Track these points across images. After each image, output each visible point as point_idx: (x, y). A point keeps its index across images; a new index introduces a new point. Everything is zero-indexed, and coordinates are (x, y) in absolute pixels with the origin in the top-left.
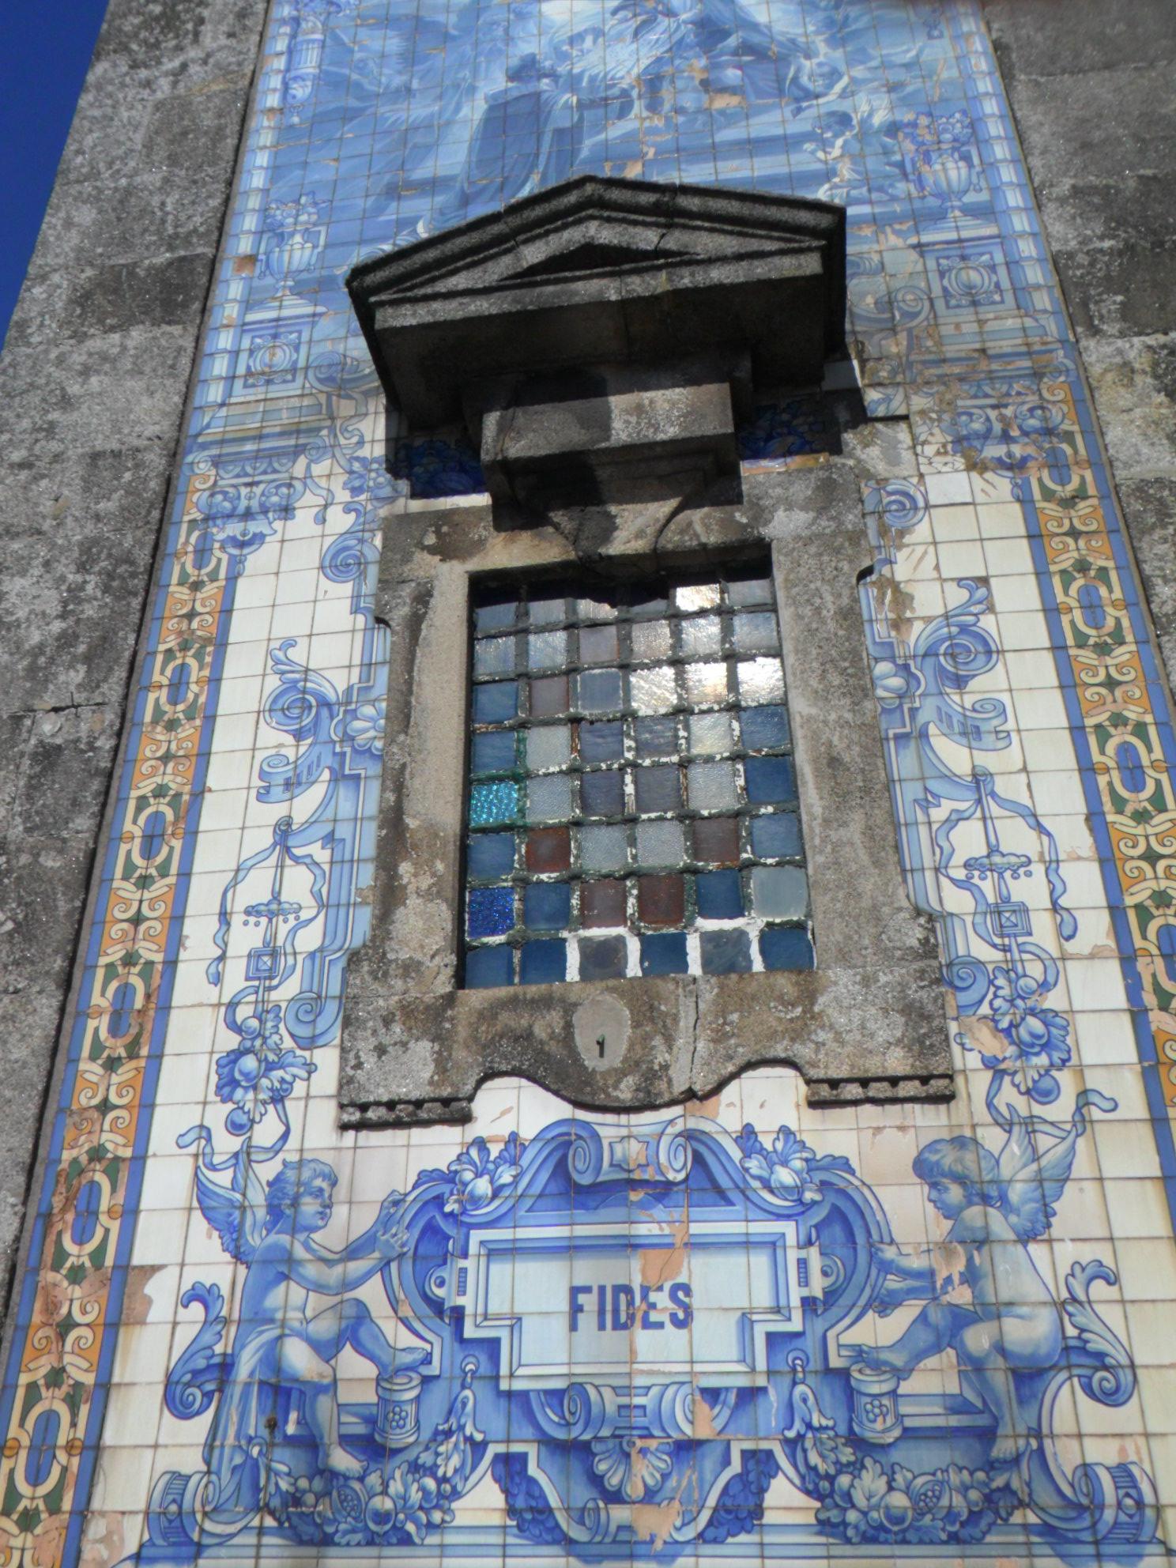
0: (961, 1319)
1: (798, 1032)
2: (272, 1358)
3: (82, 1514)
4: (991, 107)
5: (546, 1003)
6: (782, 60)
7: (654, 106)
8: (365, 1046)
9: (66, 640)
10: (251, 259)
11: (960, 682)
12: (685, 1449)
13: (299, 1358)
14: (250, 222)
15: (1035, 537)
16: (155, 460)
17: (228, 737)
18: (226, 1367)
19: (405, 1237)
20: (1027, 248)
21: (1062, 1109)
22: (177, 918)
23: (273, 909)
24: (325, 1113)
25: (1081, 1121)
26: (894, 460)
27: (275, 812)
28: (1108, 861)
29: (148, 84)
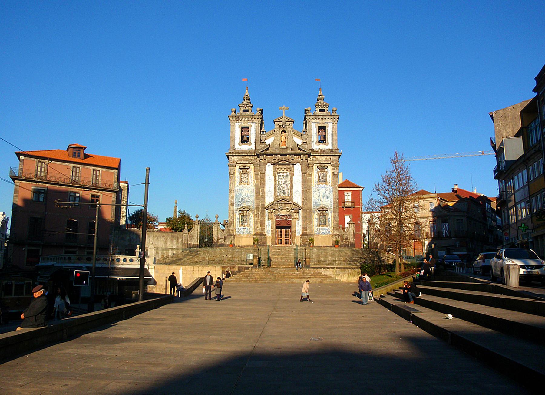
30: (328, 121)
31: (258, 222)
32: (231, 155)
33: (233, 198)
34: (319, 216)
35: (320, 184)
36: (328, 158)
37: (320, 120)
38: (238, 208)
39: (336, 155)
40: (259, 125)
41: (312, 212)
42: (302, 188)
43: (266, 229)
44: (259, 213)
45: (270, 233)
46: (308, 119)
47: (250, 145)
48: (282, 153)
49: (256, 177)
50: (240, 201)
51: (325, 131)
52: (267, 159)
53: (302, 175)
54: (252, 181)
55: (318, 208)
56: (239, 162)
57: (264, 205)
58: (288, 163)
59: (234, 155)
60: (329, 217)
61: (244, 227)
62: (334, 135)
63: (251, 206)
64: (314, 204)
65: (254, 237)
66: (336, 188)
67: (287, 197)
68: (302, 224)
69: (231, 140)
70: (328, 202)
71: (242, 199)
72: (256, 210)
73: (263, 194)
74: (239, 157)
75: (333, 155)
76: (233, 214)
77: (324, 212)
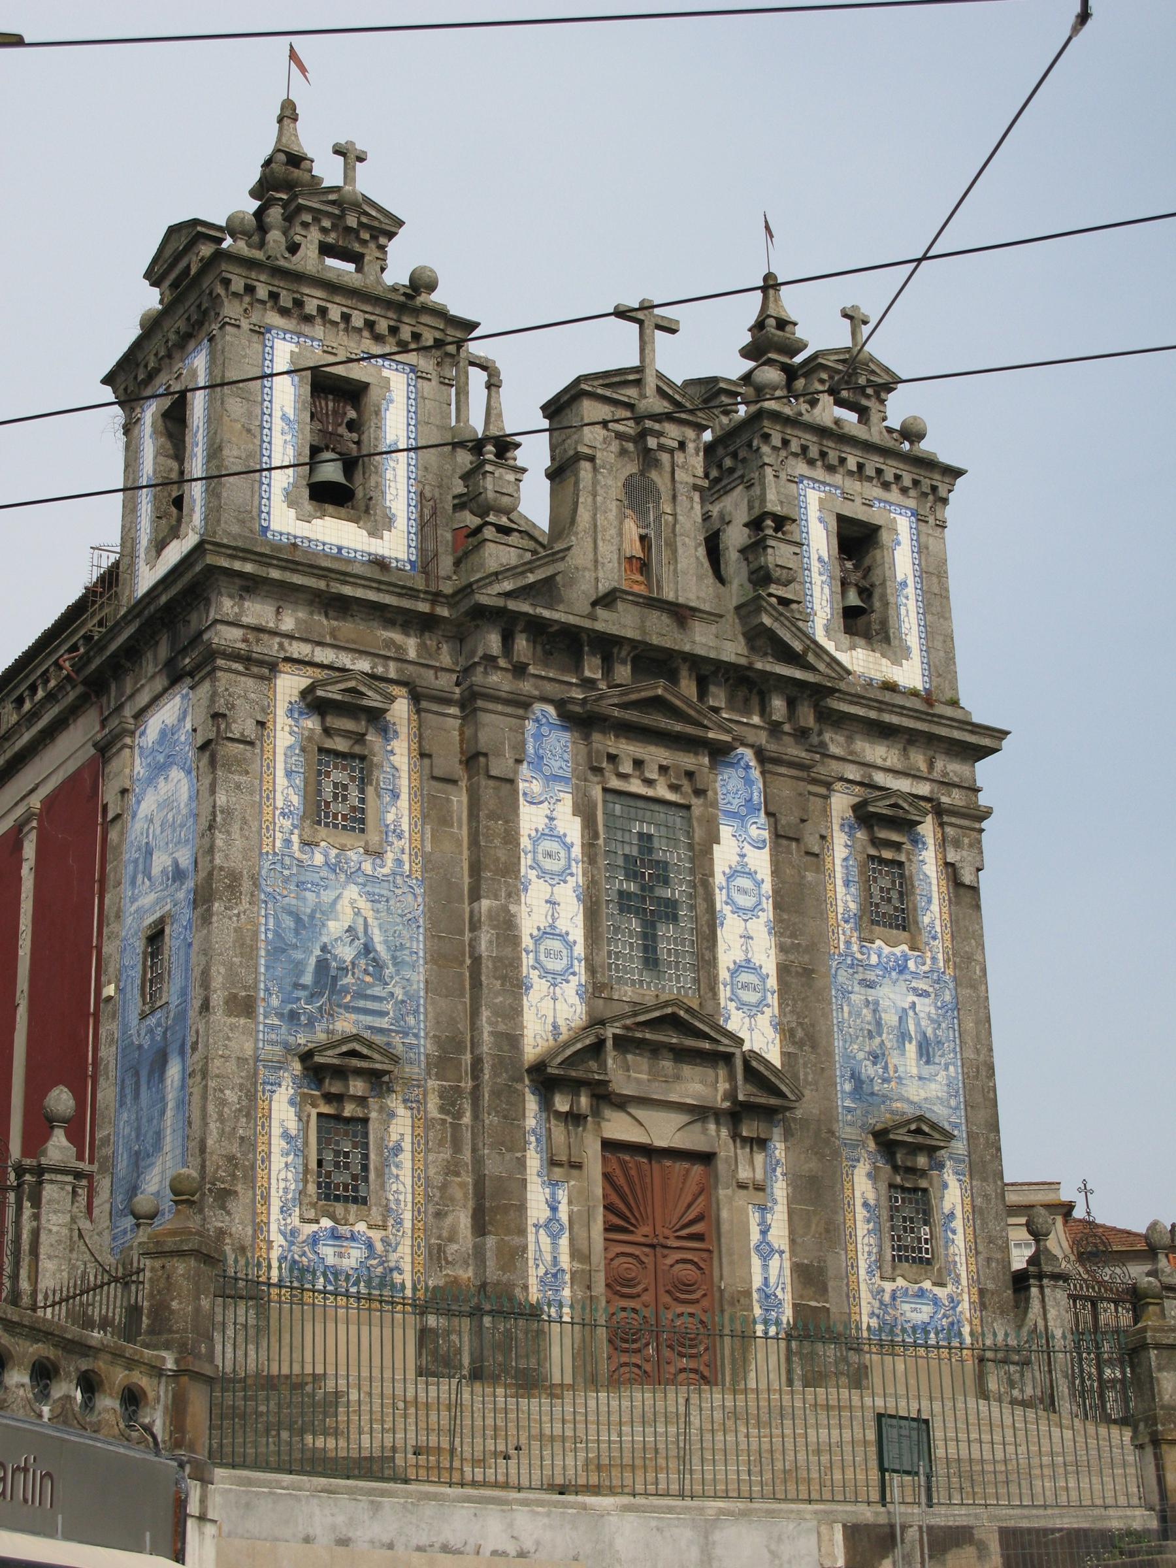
0: (384, 1262)
1: (367, 1216)
2: (293, 1257)
4: (422, 1001)
7: (353, 974)
8: (304, 1208)
9: (240, 1110)
10: (264, 999)
13: (296, 1257)
14: (262, 986)
15: (413, 1127)
16: (251, 1062)
17: (274, 1141)
19: (310, 1241)
20: (422, 1050)
21: (400, 1234)
22: (269, 1179)
23: (286, 1180)
24: (298, 1219)
28: (413, 1194)
29: (230, 918)
30: (894, 495)
31: (459, 1194)
32: (248, 568)
33: (249, 950)
34: (883, 1187)
35: (878, 942)
36: (919, 760)
37: (850, 473)
38: (288, 1048)
41: (836, 1154)
42: (782, 948)
43: (531, 1255)
44: (459, 1115)
45: (567, 1293)
46: (776, 440)
47: (374, 533)
48: (655, 640)
50: (308, 979)
52: (532, 670)
54: (405, 827)
56: (299, 650)
57: (512, 1040)
58: (690, 730)
59: (275, 574)
61: (343, 1230)
63: (397, 1040)
64: (848, 1087)
65: (432, 1321)
66: (974, 987)
68: (792, 1242)
71: (322, 966)
72: (432, 1084)
73: (508, 952)
75: (957, 735)
76: (252, 1097)
77: (922, 1161)
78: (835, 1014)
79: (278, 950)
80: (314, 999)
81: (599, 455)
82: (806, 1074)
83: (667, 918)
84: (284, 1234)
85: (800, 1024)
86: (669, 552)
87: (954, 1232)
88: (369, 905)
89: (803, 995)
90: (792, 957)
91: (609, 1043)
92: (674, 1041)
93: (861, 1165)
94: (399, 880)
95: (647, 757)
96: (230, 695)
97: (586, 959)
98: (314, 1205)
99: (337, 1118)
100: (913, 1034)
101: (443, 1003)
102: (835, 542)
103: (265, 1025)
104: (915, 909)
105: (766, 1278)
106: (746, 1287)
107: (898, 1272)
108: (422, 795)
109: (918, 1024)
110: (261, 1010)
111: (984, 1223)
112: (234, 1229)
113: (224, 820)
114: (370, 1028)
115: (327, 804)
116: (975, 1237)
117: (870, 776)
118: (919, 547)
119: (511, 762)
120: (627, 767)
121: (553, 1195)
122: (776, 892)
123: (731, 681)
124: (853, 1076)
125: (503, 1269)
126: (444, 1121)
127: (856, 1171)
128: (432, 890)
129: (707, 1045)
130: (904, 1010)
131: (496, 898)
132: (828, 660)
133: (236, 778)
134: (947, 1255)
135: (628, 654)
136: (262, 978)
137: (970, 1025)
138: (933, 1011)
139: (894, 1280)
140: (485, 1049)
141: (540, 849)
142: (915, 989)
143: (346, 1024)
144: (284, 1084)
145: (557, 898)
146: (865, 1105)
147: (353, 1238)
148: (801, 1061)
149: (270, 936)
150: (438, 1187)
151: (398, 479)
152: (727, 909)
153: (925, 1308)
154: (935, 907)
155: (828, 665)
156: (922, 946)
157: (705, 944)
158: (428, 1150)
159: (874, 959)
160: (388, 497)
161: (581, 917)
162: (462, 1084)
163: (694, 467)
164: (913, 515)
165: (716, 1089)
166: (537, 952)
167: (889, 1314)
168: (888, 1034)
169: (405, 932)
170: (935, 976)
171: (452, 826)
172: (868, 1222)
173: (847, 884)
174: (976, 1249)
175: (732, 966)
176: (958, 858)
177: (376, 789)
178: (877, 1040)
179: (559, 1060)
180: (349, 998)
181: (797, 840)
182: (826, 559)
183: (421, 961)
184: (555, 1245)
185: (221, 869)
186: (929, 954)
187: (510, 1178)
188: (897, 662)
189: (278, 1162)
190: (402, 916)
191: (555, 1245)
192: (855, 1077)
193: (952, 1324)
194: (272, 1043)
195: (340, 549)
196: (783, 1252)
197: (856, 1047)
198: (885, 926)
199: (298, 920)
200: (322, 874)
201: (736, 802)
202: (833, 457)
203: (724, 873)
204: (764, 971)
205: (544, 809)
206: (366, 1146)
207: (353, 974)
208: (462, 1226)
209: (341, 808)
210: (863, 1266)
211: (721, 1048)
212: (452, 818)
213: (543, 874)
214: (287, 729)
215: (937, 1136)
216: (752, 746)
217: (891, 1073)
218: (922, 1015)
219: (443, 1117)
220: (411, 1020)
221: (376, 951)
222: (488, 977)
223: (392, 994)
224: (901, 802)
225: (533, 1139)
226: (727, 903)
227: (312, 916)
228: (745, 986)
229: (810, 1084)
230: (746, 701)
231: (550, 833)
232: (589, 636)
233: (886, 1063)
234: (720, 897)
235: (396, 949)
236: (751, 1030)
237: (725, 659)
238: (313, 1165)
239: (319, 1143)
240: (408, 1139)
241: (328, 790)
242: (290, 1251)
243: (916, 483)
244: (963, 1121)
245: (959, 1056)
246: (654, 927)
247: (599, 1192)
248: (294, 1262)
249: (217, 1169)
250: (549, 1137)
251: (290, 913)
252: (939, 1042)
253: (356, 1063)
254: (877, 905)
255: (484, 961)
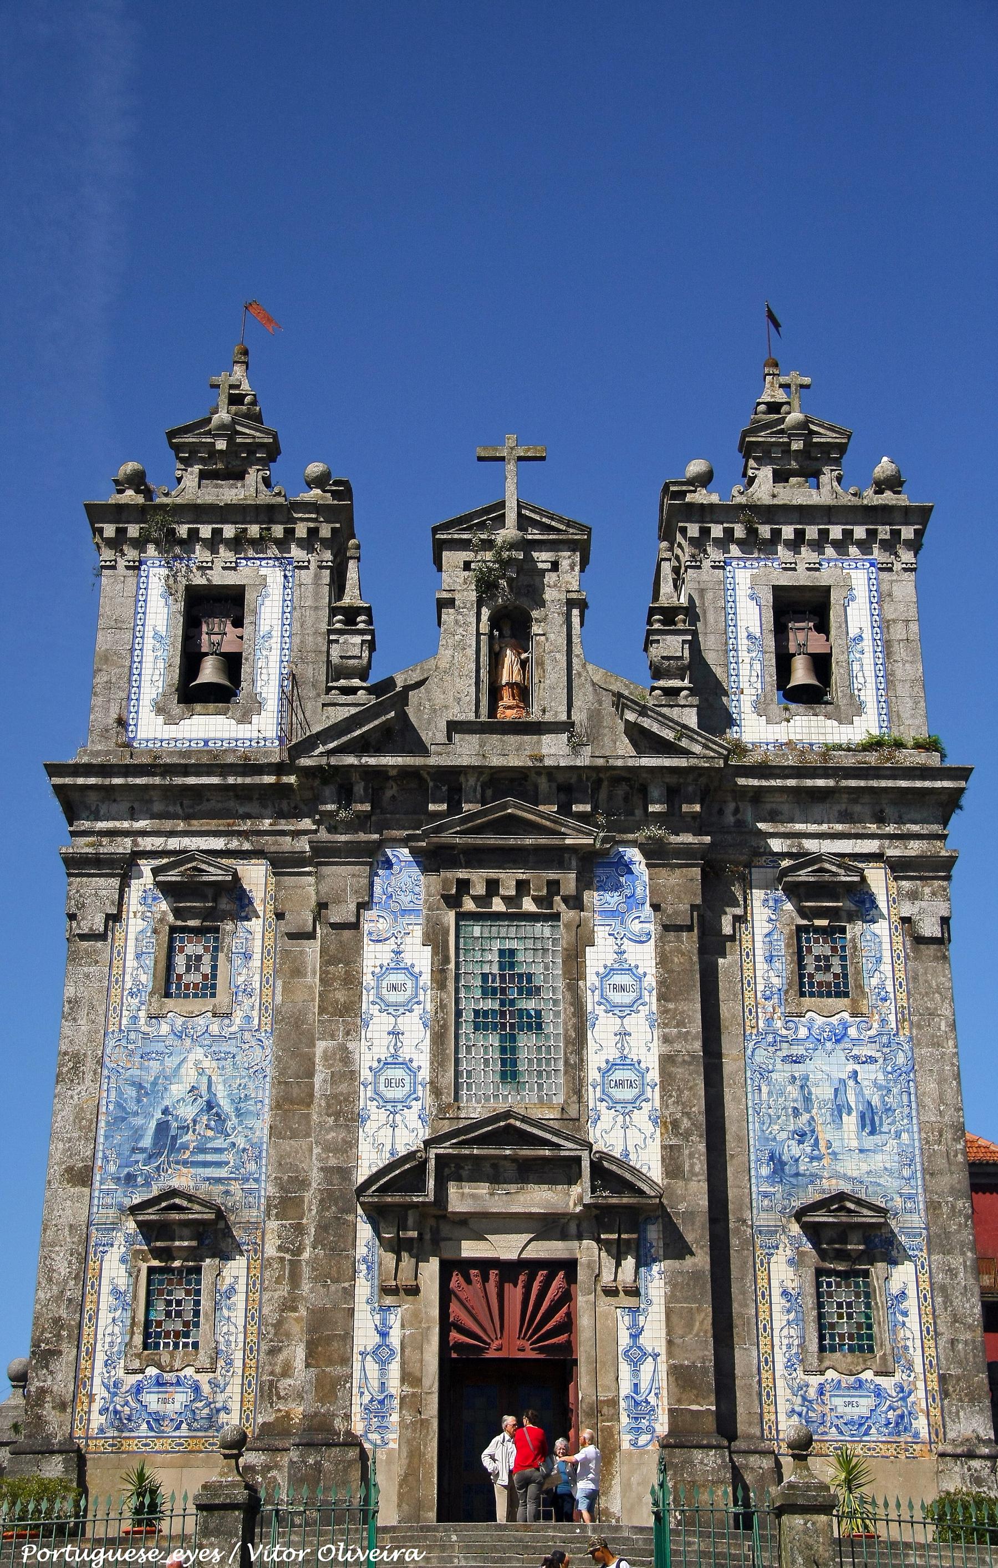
0: (211, 1403)
1: (194, 1361)
2: (115, 1407)
3: (88, 1428)
5: (156, 1354)
6: (224, 1121)
7: (194, 1131)
10: (101, 1167)
11: (230, 1298)
12: (172, 1420)
13: (118, 1407)
15: (248, 1268)
18: (108, 1409)
20: (263, 1193)
21: (230, 1374)
22: (96, 1335)
23: (112, 1334)
25: (232, 1376)
26: (227, 1247)
27: (112, 1315)
34: (809, 1274)
38: (121, 1209)
39: (927, 784)
40: (317, 577)
42: (666, 1039)
44: (299, 1251)
45: (395, 1418)
46: (693, 530)
47: (245, 719)
48: (496, 761)
49: (286, 953)
50: (147, 1142)
51: (823, 627)
53: (661, 940)
55: (797, 1204)
57: (345, 1173)
58: (543, 840)
60: (895, 1287)
62: (896, 647)
63: (235, 1187)
64: (765, 1171)
66: (937, 1044)
67: (536, 1114)
68: (670, 1343)
69: (101, 679)
70: (878, 1161)
71: (162, 1128)
72: (273, 1225)
73: (343, 1087)
74: (157, 807)
76: (84, 1260)
78: (750, 1095)
79: (120, 1118)
80: (152, 1160)
81: (457, 596)
82: (692, 1166)
83: (530, 1027)
84: (107, 1388)
85: (688, 1114)
86: (540, 671)
87: (905, 1314)
88: (214, 1064)
89: (691, 1084)
90: (677, 1046)
91: (432, 1164)
92: (508, 1152)
93: (781, 1249)
94: (247, 1036)
95: (501, 876)
96: (80, 896)
97: (431, 1083)
98: (139, 1356)
99: (170, 1270)
100: (854, 1107)
101: (287, 1145)
102: (769, 615)
103: (101, 1191)
104: (858, 972)
105: (636, 1385)
106: (610, 1395)
107: (827, 1363)
108: (275, 953)
109: (860, 1094)
110: (98, 1178)
111: (947, 1300)
112: (55, 1388)
113: (71, 1009)
114: (208, 1179)
115: (180, 977)
116: (935, 1317)
117: (800, 845)
118: (880, 597)
119: (353, 907)
120: (479, 889)
121: (384, 1321)
122: (661, 983)
123: (606, 783)
124: (772, 1158)
125: (322, 1400)
126: (282, 1259)
127: (773, 1259)
128: (281, 1039)
129: (547, 1153)
130: (843, 1081)
131: (333, 1037)
132: (704, 741)
133: (86, 969)
134: (895, 1340)
135: (478, 780)
136: (101, 1148)
137: (931, 1086)
138: (881, 1076)
139: (822, 1373)
140: (314, 1185)
141: (384, 984)
142: (856, 1058)
143: (182, 1180)
144: (116, 1243)
145: (401, 1027)
146: (788, 1187)
147: (178, 1383)
148: (687, 1152)
149: (111, 1107)
150: (273, 1325)
151: (271, 664)
152: (600, 1010)
153: (863, 1401)
154: (886, 968)
155: (706, 747)
156: (865, 1010)
157: (570, 1048)
158: (264, 1289)
159: (803, 1032)
160: (259, 684)
161: (427, 1041)
162: (304, 1221)
163: (567, 582)
164: (872, 565)
165: (570, 1196)
166: (376, 1083)
167: (814, 1410)
168: (820, 1108)
169: (251, 1085)
170: (885, 1039)
171: (305, 976)
172: (789, 1311)
173: (770, 959)
174: (935, 1331)
175: (603, 1065)
176: (916, 910)
177: (227, 955)
178: (805, 1117)
179: (374, 1188)
180: (188, 1153)
181: (690, 928)
182: (758, 635)
183: (267, 1109)
184: (383, 1371)
185: (65, 1054)
186: (877, 1017)
187: (335, 1307)
188: (844, 719)
189: (105, 1318)
190: (248, 1069)
191: (383, 1371)
192: (776, 1160)
193: (902, 1417)
194: (107, 1206)
195: (206, 742)
196: (656, 1356)
197: (776, 1127)
198: (821, 995)
199: (140, 1087)
200: (167, 1043)
201: (613, 901)
202: (765, 531)
203: (597, 974)
204: (643, 1065)
205: (391, 945)
206: (198, 1292)
207: (194, 1131)
208: (297, 1359)
209: (194, 978)
210: (780, 1361)
211: (563, 1153)
212: (306, 968)
213: (387, 1007)
214: (139, 915)
215: (866, 1212)
216: (634, 843)
217: (823, 1150)
218: (865, 1083)
219: (282, 1255)
220: (252, 1167)
221: (219, 1106)
222: (320, 1114)
223: (234, 1144)
224: (827, 866)
225: (363, 1267)
226: (600, 1004)
227: (154, 1084)
228: (619, 1084)
229: (697, 1175)
230: (626, 799)
231: (398, 965)
232: (428, 773)
233: (817, 1140)
234: (591, 1000)
235: (238, 1102)
236: (625, 1127)
237: (578, 763)
238: (141, 1317)
239: (149, 1293)
240: (242, 1281)
241: (180, 961)
242: (112, 1402)
243: (872, 534)
244: (920, 1191)
245: (915, 1121)
246: (513, 1038)
247: (435, 1312)
248: (116, 1412)
249: (42, 1333)
250: (380, 1264)
251: (133, 1084)
252: (890, 1109)
253: (176, 1216)
254: (811, 976)
255: (316, 1101)
